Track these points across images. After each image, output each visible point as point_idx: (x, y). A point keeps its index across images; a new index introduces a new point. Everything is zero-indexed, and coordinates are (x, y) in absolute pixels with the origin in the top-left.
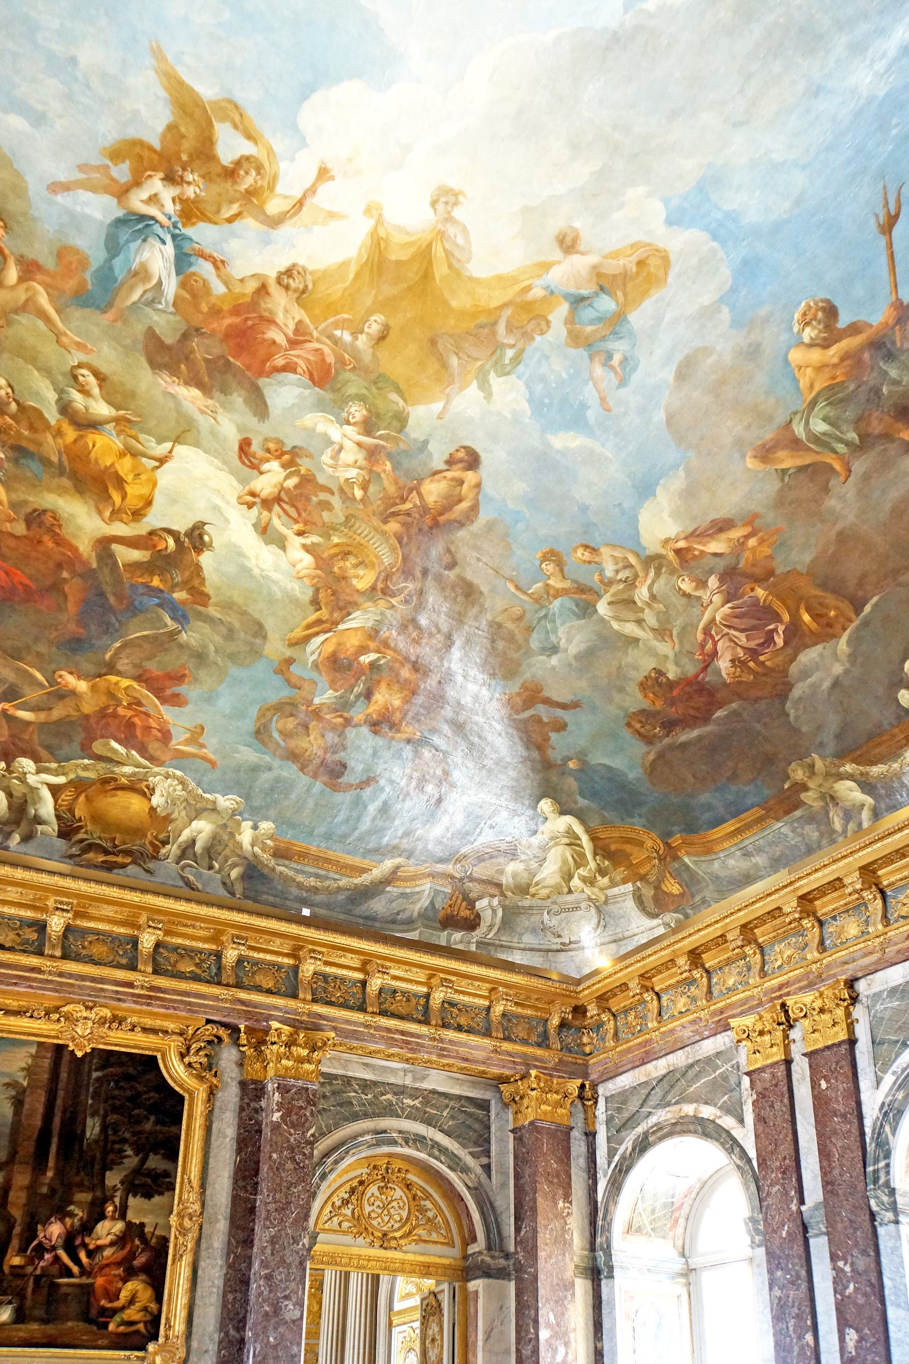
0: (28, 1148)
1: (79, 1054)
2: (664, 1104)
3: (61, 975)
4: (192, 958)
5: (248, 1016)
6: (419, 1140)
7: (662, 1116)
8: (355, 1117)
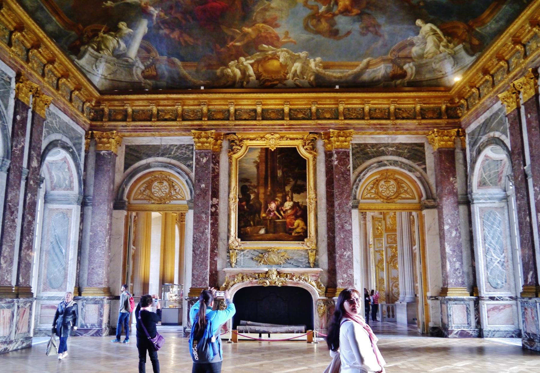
0: (262, 181)
1: (273, 150)
2: (485, 133)
3: (262, 125)
4: (302, 112)
5: (323, 129)
6: (395, 163)
7: (484, 138)
8: (370, 158)
